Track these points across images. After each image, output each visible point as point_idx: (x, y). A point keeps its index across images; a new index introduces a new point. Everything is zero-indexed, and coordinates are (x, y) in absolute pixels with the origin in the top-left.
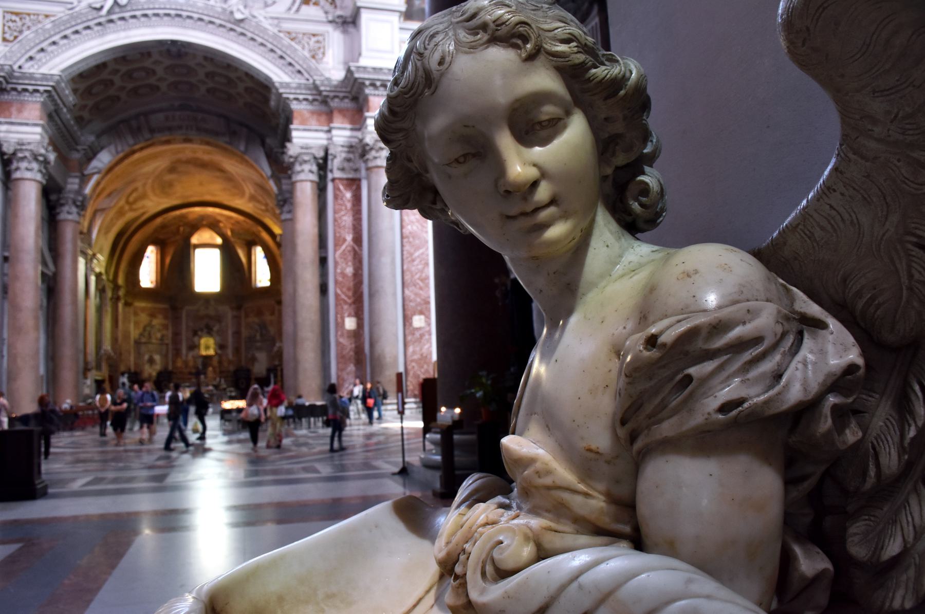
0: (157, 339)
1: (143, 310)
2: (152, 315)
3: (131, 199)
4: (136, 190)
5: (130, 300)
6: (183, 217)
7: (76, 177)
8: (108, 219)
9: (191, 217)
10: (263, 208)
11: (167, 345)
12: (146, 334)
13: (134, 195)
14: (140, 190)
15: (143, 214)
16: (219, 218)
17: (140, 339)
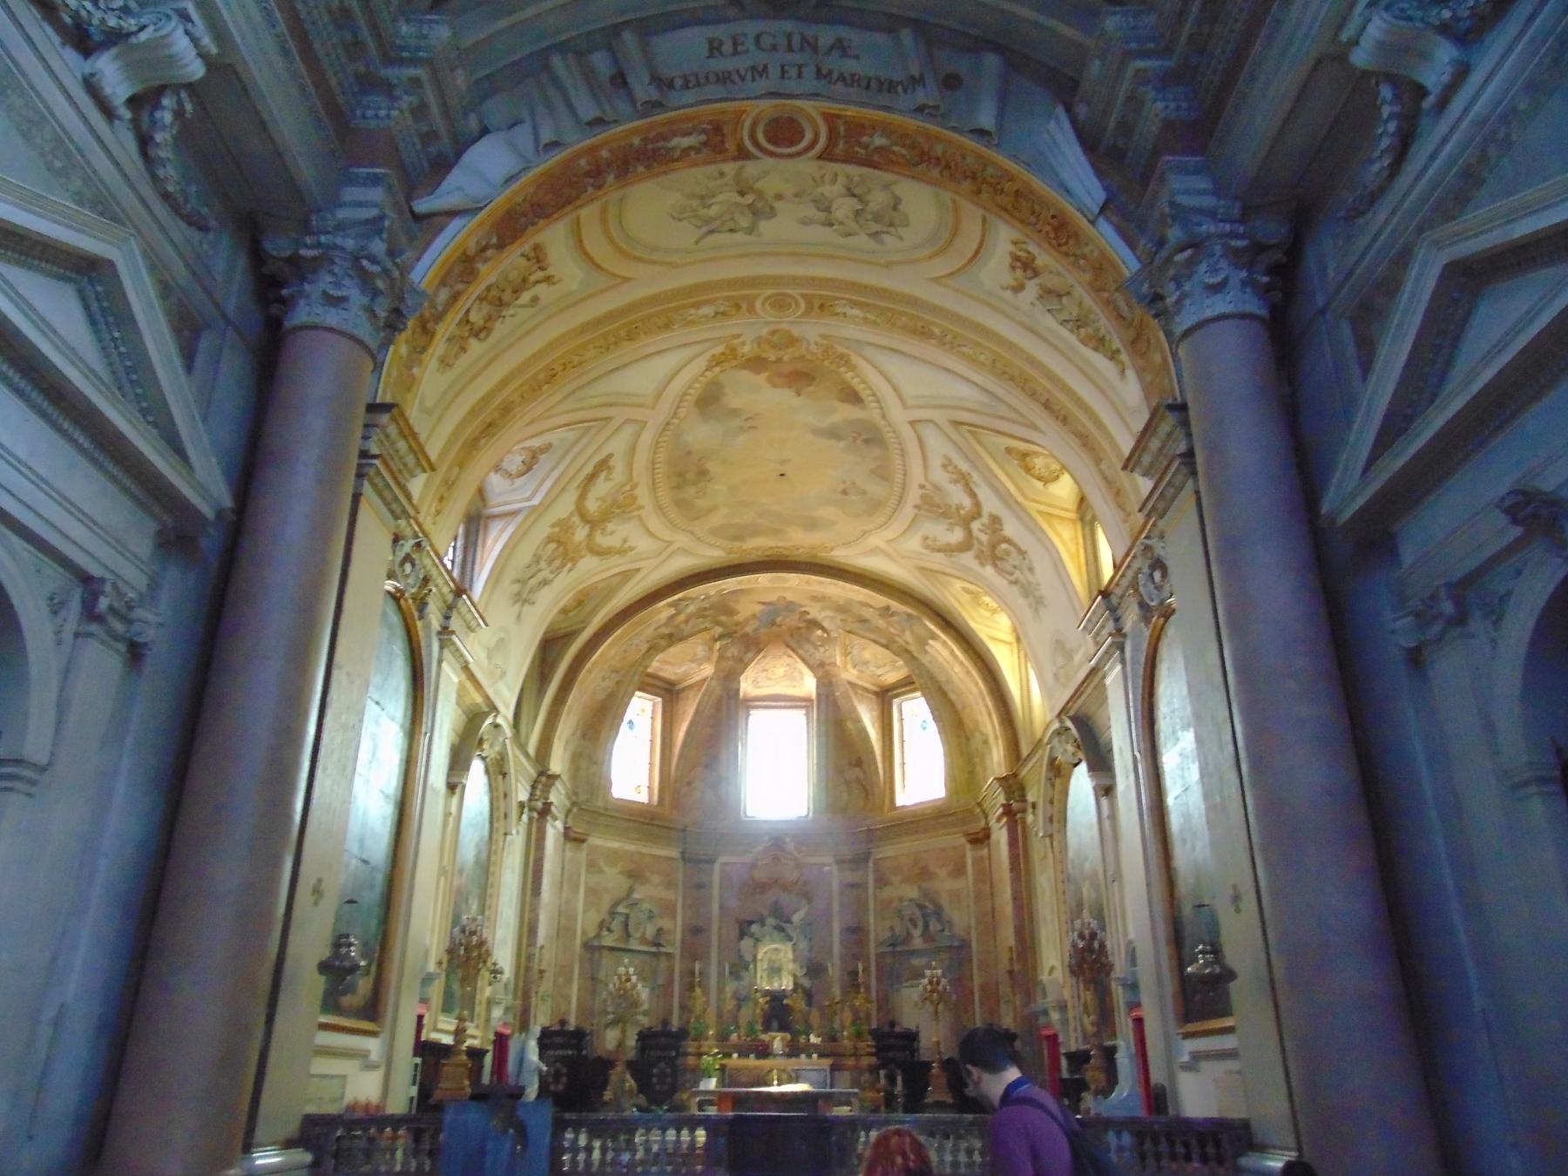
0: (643, 940)
1: (613, 857)
2: (635, 875)
3: (592, 505)
4: (604, 465)
5: (579, 829)
6: (724, 607)
7: (376, 180)
8: (525, 554)
9: (746, 609)
10: (957, 536)
11: (669, 956)
12: (616, 925)
13: (601, 488)
14: (618, 465)
15: (626, 576)
16: (815, 612)
17: (598, 936)
